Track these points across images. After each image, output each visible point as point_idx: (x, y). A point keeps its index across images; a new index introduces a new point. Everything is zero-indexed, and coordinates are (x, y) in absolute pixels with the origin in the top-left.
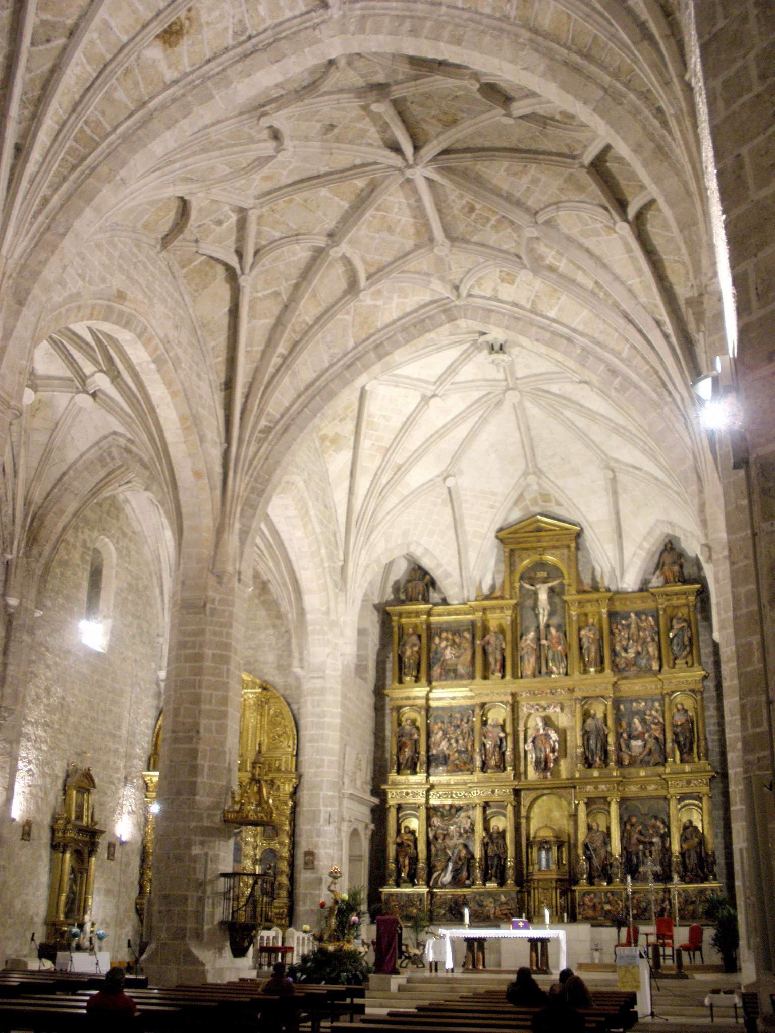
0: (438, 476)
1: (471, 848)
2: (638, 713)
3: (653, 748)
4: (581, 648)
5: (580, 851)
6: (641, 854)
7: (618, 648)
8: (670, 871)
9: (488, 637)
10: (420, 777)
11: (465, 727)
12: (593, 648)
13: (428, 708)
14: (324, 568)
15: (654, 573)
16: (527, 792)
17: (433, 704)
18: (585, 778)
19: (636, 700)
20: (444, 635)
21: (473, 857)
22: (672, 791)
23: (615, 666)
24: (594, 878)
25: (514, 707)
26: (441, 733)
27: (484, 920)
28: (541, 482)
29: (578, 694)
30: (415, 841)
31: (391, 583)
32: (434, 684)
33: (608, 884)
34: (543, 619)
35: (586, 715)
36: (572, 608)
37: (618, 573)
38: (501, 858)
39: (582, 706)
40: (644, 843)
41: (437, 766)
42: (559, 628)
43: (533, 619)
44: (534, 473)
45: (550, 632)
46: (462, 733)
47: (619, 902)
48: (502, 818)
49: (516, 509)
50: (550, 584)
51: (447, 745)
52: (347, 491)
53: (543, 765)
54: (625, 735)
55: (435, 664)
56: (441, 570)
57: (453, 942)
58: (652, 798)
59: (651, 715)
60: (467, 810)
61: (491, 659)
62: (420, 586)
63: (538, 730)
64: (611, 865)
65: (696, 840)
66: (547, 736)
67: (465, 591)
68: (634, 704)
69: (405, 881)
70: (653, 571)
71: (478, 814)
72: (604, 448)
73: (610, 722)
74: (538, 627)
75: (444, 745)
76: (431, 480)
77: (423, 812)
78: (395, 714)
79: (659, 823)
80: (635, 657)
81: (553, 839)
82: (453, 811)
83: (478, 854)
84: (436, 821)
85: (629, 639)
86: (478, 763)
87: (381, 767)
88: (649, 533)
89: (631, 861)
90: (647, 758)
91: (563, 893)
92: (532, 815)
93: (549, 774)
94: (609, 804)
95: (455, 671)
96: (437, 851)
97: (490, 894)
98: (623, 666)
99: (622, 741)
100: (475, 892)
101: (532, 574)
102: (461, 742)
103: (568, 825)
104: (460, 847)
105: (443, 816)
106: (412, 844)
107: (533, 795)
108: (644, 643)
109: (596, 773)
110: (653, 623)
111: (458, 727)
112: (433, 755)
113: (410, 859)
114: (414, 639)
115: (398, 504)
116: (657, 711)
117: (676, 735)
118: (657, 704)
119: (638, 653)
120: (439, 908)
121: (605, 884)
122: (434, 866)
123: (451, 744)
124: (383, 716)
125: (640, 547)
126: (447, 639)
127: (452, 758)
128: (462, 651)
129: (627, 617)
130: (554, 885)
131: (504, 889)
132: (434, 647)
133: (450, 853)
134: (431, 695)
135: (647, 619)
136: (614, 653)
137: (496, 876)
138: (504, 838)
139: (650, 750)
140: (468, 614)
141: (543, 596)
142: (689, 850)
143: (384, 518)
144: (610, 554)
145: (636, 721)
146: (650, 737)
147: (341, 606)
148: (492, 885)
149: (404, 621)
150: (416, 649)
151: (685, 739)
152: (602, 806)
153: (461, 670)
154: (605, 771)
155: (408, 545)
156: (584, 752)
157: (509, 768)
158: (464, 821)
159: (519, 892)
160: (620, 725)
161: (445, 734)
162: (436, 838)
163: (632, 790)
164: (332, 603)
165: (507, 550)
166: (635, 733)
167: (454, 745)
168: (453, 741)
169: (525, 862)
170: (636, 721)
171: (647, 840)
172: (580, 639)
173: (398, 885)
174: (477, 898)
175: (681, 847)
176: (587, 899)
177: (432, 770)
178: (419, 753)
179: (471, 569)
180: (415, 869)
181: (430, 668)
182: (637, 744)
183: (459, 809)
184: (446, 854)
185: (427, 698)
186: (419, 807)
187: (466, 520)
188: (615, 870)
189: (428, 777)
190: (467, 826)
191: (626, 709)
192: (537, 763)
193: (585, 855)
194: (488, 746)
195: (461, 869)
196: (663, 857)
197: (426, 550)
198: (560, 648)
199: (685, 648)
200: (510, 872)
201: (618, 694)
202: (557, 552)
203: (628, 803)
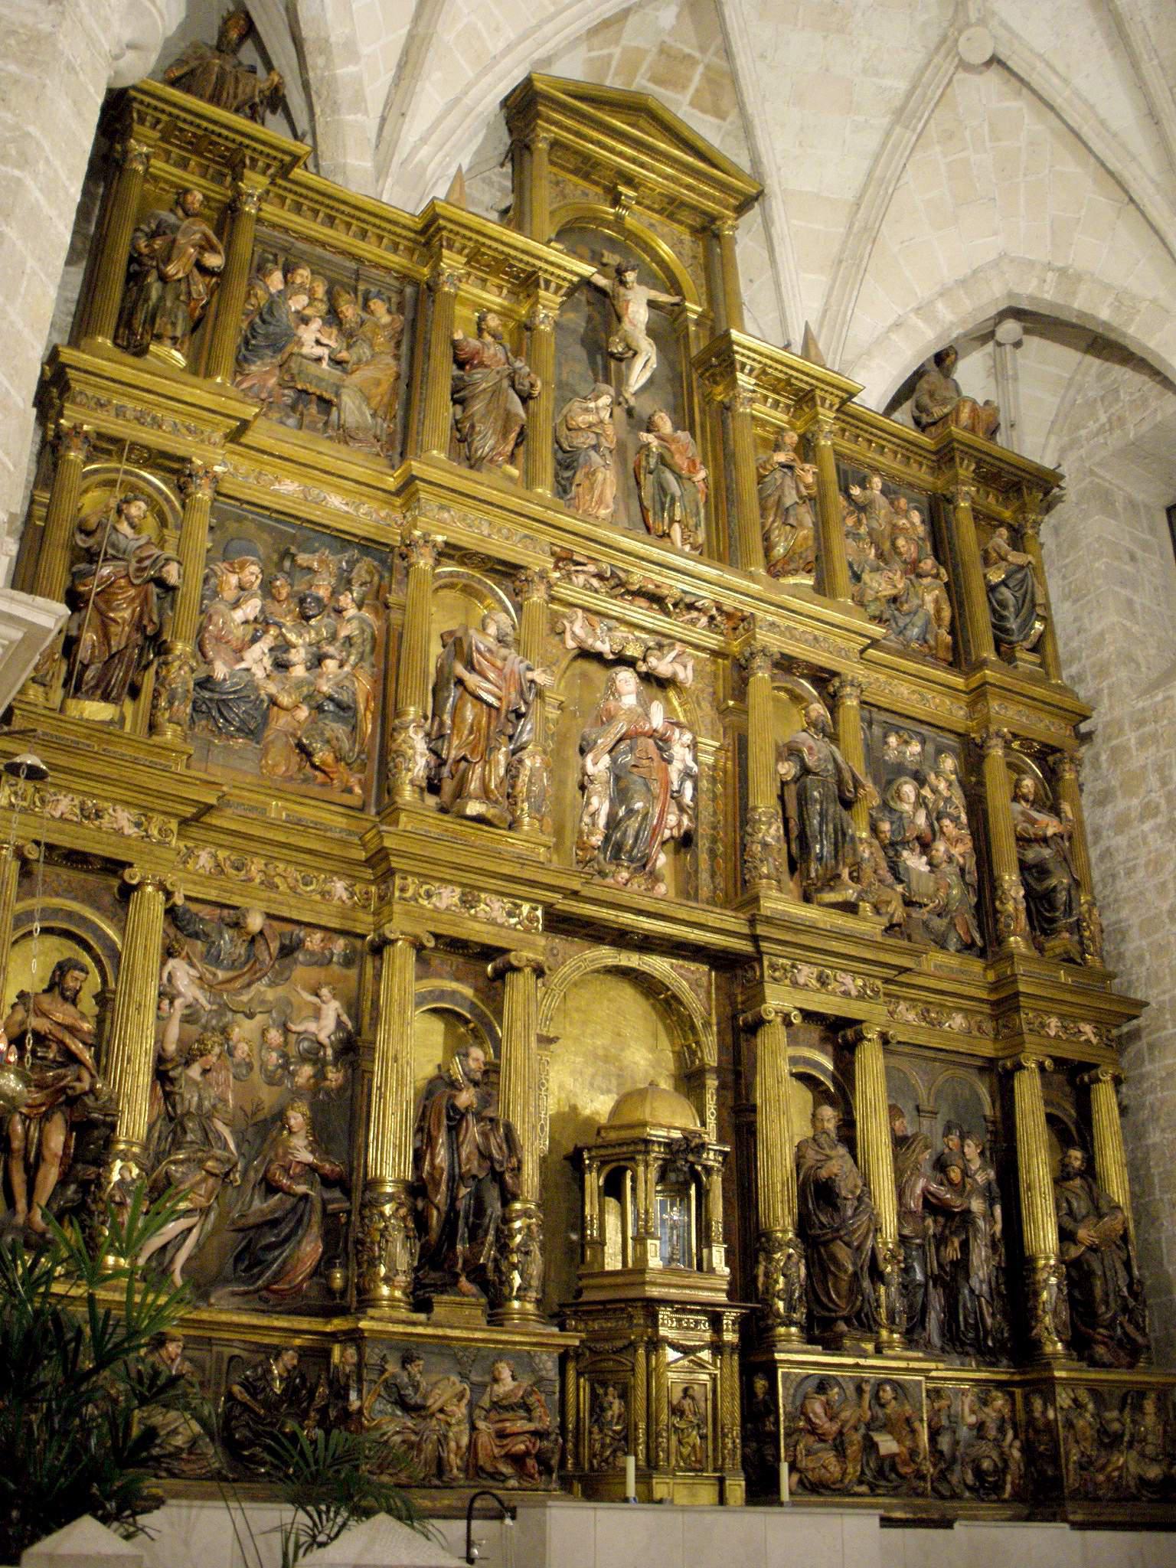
49: (582, 52)
56: (352, 69)
75: (257, 658)
88: (963, 283)
102: (331, 665)
127: (281, 721)
128: (364, 351)
153: (352, 409)
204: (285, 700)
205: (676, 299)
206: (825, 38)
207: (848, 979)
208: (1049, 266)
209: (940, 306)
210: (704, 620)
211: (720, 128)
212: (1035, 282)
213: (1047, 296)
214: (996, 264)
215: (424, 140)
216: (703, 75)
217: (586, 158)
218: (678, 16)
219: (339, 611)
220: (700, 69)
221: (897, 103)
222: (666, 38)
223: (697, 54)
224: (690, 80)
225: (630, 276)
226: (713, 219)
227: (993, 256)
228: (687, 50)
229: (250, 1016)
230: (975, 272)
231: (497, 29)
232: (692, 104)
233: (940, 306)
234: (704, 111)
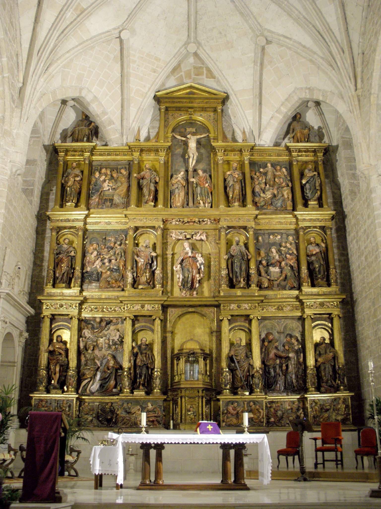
0: (115, 29)
1: (119, 359)
2: (274, 244)
3: (289, 274)
4: (225, 188)
5: (224, 364)
6: (277, 367)
7: (257, 189)
8: (305, 382)
9: (142, 173)
10: (74, 291)
11: (118, 249)
12: (238, 187)
13: (85, 231)
14: (3, 77)
15: (284, 139)
16: (173, 310)
17: (88, 227)
18: (230, 296)
19: (273, 234)
20: (103, 171)
21: (121, 368)
22: (308, 312)
23: (255, 204)
24: (237, 388)
25: (165, 231)
26: (95, 253)
27: (131, 427)
28: (199, 52)
29: (224, 223)
30: (67, 351)
31: (60, 131)
32: (92, 211)
33: (250, 394)
34: (192, 163)
35: (229, 244)
36: (219, 154)
37: (256, 133)
38: (150, 368)
39: (227, 234)
40: (280, 357)
41: (90, 282)
42: (204, 171)
43: (182, 164)
44: (194, 43)
45: (198, 174)
46: (115, 254)
47: (261, 410)
48: (150, 333)
50: (198, 137)
51: (100, 264)
52: (33, 20)
53: (189, 285)
54: (264, 262)
55: (93, 194)
57: (126, 447)
58: (286, 318)
59: (286, 247)
60: (117, 324)
61: (145, 191)
62: (86, 131)
63: (187, 253)
64: (253, 376)
65: (331, 354)
66: (194, 258)
67: (125, 137)
68: (271, 237)
69: (55, 388)
70: (282, 137)
71: (128, 325)
72: (260, 21)
73: (252, 248)
74: (187, 171)
75: (98, 263)
76: (108, 32)
77: (75, 322)
78: (54, 234)
79: (294, 341)
80: (272, 199)
81: (199, 351)
82: (103, 324)
83: (126, 365)
84: (87, 332)
85: (266, 184)
86: (130, 280)
87: (38, 283)
88: (286, 100)
89: (269, 373)
90: (283, 283)
91: (208, 402)
92: (176, 331)
93: (195, 293)
94: (250, 321)
95: (111, 200)
96: (86, 361)
97: (137, 402)
98: (263, 204)
99: (261, 266)
100: (121, 400)
101: (183, 130)
102: (113, 261)
103: (211, 341)
104: (109, 358)
105: (93, 328)
106: (63, 352)
107: (178, 311)
108: (280, 187)
109: (239, 292)
110: (286, 173)
111: (112, 248)
112: (87, 272)
113: (61, 366)
114: (77, 171)
115: (77, 46)
116: (291, 244)
117: (309, 264)
118: (291, 238)
119: (275, 196)
120: (87, 414)
121: (247, 393)
122: (84, 374)
123: (104, 264)
124: (43, 239)
125: (278, 111)
126: (106, 175)
127: (104, 276)
128: (119, 184)
129: (265, 166)
130: (200, 394)
131: (150, 397)
132: (94, 180)
133: (99, 363)
134: (89, 220)
135: (280, 170)
136: (253, 192)
137: (143, 385)
138: (152, 350)
139: (286, 277)
140: (125, 155)
141: (192, 144)
142: (324, 363)
143: (63, 55)
144: (250, 118)
145: (274, 250)
146: (286, 265)
147: (16, 120)
148: (140, 394)
149: (69, 158)
150: (78, 179)
151: (320, 267)
152: (243, 324)
153: (117, 200)
154: (246, 291)
155: (81, 90)
156: (228, 274)
157: (158, 286)
158: (113, 333)
159: (165, 400)
160: (259, 254)
161: (99, 254)
162: (86, 348)
163: (271, 311)
164: (7, 114)
165: (163, 107)
166: (273, 261)
167: (107, 264)
168: (106, 261)
169: (169, 373)
170: (274, 250)
171: (283, 355)
172: (225, 180)
173: (48, 392)
174: (125, 405)
175: (316, 361)
176: (230, 408)
177: (85, 287)
178: (74, 269)
179: (131, 122)
180: (65, 376)
181: (89, 197)
182: (275, 270)
183: (109, 323)
184: (95, 364)
185: (85, 224)
186: (71, 318)
187: (132, 79)
188: (256, 380)
189: (82, 291)
190: (116, 338)
191: (263, 240)
192: (184, 283)
193: (229, 366)
194: (140, 265)
195: (109, 377)
196: (298, 371)
197: (95, 97)
198: (207, 185)
199: (316, 192)
200: (157, 382)
201: (258, 227)
202: (204, 114)
203: (267, 322)
204: (104, 271)
205: (207, 134)
206: (229, 50)
207: (246, 306)
208: (306, 88)
209: (282, 108)
210: (209, 223)
211: (215, 81)
212: (304, 94)
213: (308, 97)
214: (294, 92)
215: (133, 121)
216: (206, 70)
217: (177, 107)
218: (194, 59)
219: (116, 247)
220: (205, 69)
221: (253, 59)
222: (195, 65)
223: (202, 66)
224: (203, 72)
225: (188, 136)
226: (216, 108)
227: (293, 89)
228: (200, 66)
229: (102, 338)
230: (289, 95)
231: (145, 86)
232: (207, 77)
233: (282, 108)
234: (210, 78)
